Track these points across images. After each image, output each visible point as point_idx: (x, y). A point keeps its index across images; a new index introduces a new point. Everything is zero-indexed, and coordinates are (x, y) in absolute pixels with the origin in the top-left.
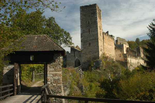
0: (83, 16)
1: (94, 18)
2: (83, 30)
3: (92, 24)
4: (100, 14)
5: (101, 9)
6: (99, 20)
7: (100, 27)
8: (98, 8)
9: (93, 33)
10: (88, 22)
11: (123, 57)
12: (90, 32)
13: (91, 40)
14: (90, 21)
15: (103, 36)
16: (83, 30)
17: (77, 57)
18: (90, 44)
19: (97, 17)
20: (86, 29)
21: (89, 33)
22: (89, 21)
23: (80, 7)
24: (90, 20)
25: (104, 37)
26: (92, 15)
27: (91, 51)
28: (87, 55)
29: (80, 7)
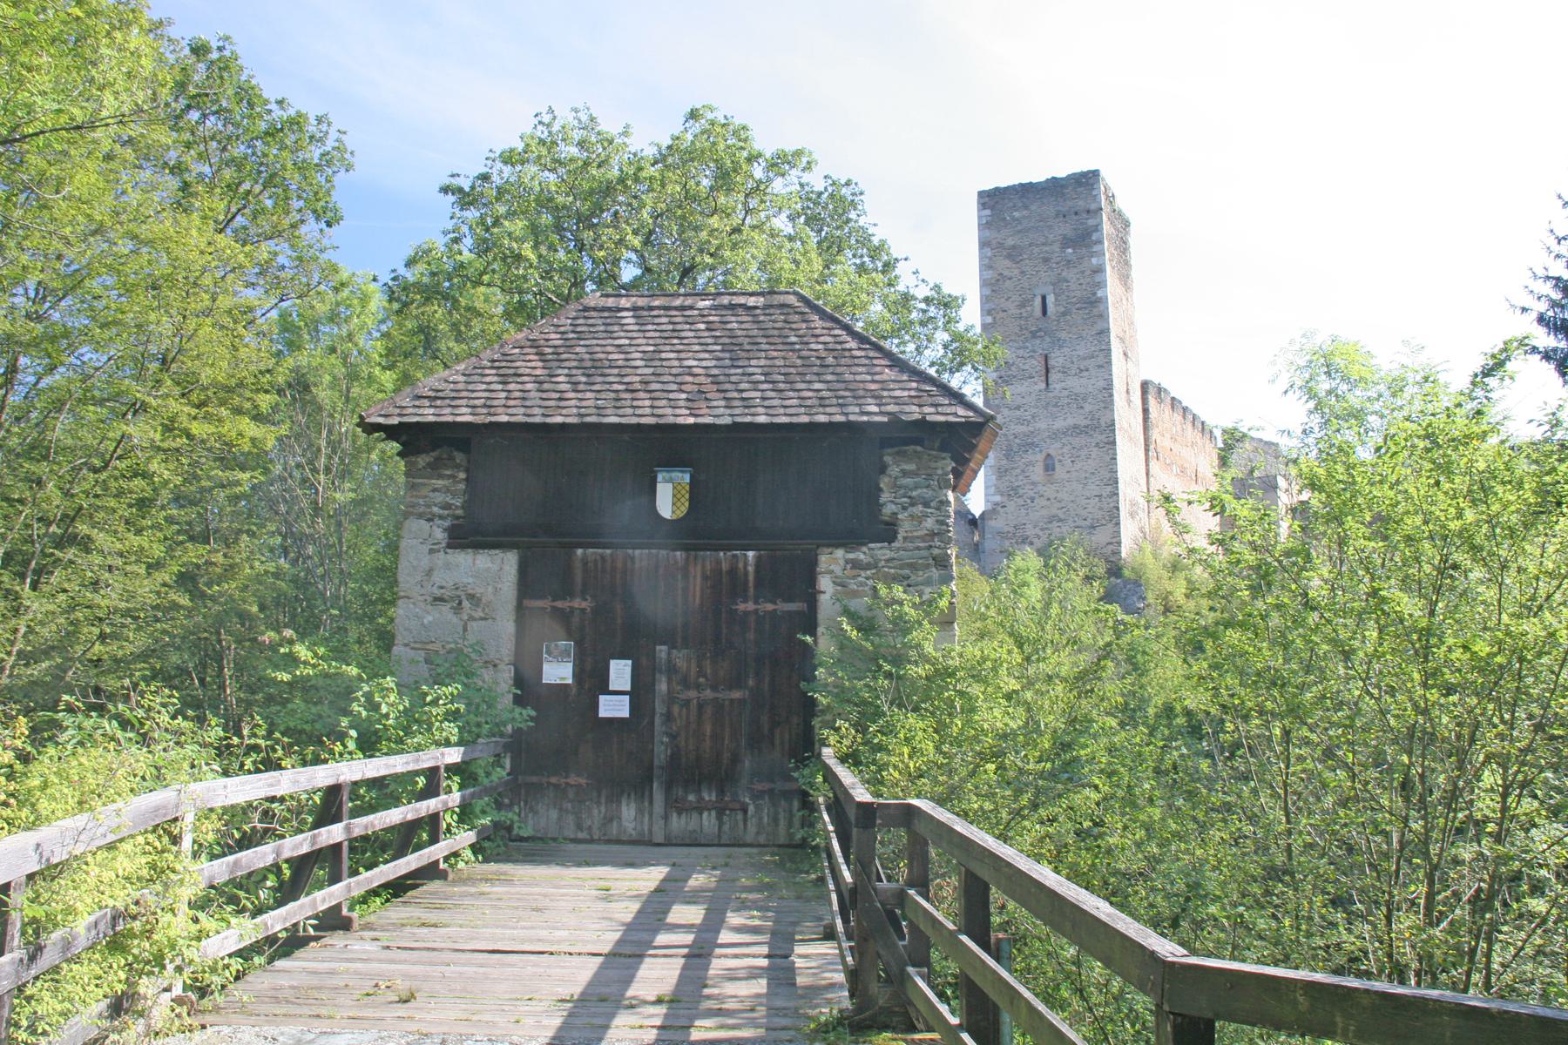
0: (1003, 264)
1: (1083, 272)
3: (1064, 314)
4: (1123, 247)
5: (1128, 213)
7: (1122, 340)
8: (1111, 199)
9: (1072, 382)
10: (1038, 301)
12: (1053, 377)
13: (1055, 435)
14: (1050, 299)
15: (1146, 411)
19: (1099, 270)
20: (1021, 352)
21: (1043, 386)
22: (1044, 298)
23: (981, 194)
26: (1070, 250)
27: (1060, 514)
29: (981, 194)
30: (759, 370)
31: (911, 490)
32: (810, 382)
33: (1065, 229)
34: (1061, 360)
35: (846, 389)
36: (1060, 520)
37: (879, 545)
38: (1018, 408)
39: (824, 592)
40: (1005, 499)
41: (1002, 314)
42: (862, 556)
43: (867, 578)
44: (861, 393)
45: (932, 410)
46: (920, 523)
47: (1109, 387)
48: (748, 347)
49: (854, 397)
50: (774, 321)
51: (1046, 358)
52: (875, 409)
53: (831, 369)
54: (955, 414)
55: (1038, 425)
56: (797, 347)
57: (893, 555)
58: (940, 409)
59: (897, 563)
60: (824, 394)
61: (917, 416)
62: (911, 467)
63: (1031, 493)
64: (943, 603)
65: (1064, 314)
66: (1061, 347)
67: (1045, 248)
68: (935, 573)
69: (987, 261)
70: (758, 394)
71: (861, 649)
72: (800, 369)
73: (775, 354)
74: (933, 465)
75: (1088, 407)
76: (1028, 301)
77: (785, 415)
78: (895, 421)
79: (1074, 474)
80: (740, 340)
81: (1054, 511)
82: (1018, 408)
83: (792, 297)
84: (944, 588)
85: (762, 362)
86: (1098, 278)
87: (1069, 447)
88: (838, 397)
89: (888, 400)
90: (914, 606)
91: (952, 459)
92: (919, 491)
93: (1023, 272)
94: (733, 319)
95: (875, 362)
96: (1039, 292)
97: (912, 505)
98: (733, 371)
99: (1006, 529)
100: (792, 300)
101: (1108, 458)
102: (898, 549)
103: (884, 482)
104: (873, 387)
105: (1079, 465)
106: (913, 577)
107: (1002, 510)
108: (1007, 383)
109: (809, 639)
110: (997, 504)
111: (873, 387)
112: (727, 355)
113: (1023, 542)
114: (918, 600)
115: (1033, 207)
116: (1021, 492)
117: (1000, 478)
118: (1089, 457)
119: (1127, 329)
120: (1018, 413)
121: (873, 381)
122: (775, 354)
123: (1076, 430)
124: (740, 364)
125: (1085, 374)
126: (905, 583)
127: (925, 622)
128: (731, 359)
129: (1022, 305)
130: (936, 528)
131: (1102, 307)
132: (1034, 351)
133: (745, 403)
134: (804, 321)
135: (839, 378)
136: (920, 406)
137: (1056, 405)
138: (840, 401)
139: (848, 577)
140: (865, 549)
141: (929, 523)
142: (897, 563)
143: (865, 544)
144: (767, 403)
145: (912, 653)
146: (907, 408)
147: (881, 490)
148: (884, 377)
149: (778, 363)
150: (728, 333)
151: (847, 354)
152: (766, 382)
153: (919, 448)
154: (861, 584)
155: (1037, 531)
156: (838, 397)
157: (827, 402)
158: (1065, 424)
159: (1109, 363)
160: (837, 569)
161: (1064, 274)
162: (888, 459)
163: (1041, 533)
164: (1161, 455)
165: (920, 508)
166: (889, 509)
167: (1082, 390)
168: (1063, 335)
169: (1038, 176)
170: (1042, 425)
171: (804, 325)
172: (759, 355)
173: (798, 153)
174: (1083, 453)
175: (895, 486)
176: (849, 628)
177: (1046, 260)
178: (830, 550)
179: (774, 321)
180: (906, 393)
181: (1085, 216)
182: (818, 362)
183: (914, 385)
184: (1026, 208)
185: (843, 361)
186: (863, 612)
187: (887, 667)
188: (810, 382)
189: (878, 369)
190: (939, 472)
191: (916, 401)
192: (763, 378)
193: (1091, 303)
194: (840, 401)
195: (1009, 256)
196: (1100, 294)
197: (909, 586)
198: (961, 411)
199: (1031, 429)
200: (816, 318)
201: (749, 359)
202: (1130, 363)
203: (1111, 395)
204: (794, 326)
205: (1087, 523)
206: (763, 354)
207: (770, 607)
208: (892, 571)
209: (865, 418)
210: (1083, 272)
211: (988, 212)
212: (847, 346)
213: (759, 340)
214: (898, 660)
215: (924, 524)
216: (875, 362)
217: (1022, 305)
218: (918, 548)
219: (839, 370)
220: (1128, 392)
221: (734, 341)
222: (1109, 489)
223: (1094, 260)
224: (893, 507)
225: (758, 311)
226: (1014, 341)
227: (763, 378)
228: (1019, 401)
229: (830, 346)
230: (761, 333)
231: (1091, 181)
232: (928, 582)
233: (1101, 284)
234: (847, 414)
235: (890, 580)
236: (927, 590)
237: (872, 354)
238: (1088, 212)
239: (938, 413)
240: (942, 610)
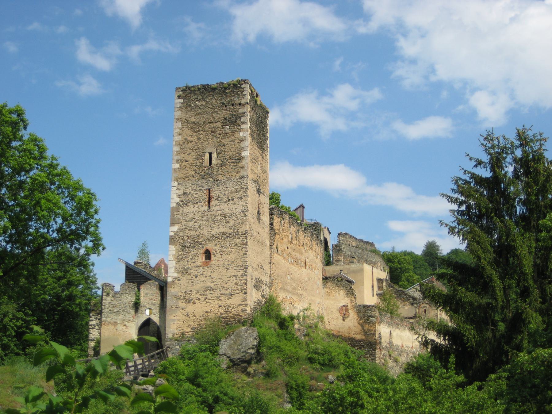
0: (187, 132)
1: (233, 141)
2: (185, 193)
7: (256, 182)
10: (207, 156)
11: (356, 317)
12: (213, 203)
14: (214, 155)
15: (271, 224)
16: (185, 193)
17: (147, 312)
18: (208, 254)
20: (195, 187)
21: (207, 208)
22: (210, 154)
24: (213, 150)
26: (228, 127)
27: (212, 285)
28: (194, 303)
33: (224, 113)
34: (218, 193)
36: (212, 290)
38: (191, 220)
40: (180, 275)
41: (185, 163)
51: (209, 190)
55: (202, 232)
63: (196, 273)
75: (232, 222)
79: (222, 262)
81: (209, 284)
82: (191, 220)
93: (199, 138)
99: (180, 294)
105: (224, 257)
108: (185, 205)
110: (175, 278)
113: (189, 302)
116: (190, 271)
117: (178, 262)
120: (191, 223)
125: (231, 202)
137: (213, 220)
155: (198, 295)
158: (218, 231)
163: (200, 297)
164: (280, 252)
167: (229, 212)
168: (220, 178)
170: (204, 232)
177: (213, 132)
184: (204, 99)
199: (198, 234)
205: (228, 292)
210: (233, 141)
222: (242, 272)
228: (191, 216)
231: (243, 86)
238: (240, 104)
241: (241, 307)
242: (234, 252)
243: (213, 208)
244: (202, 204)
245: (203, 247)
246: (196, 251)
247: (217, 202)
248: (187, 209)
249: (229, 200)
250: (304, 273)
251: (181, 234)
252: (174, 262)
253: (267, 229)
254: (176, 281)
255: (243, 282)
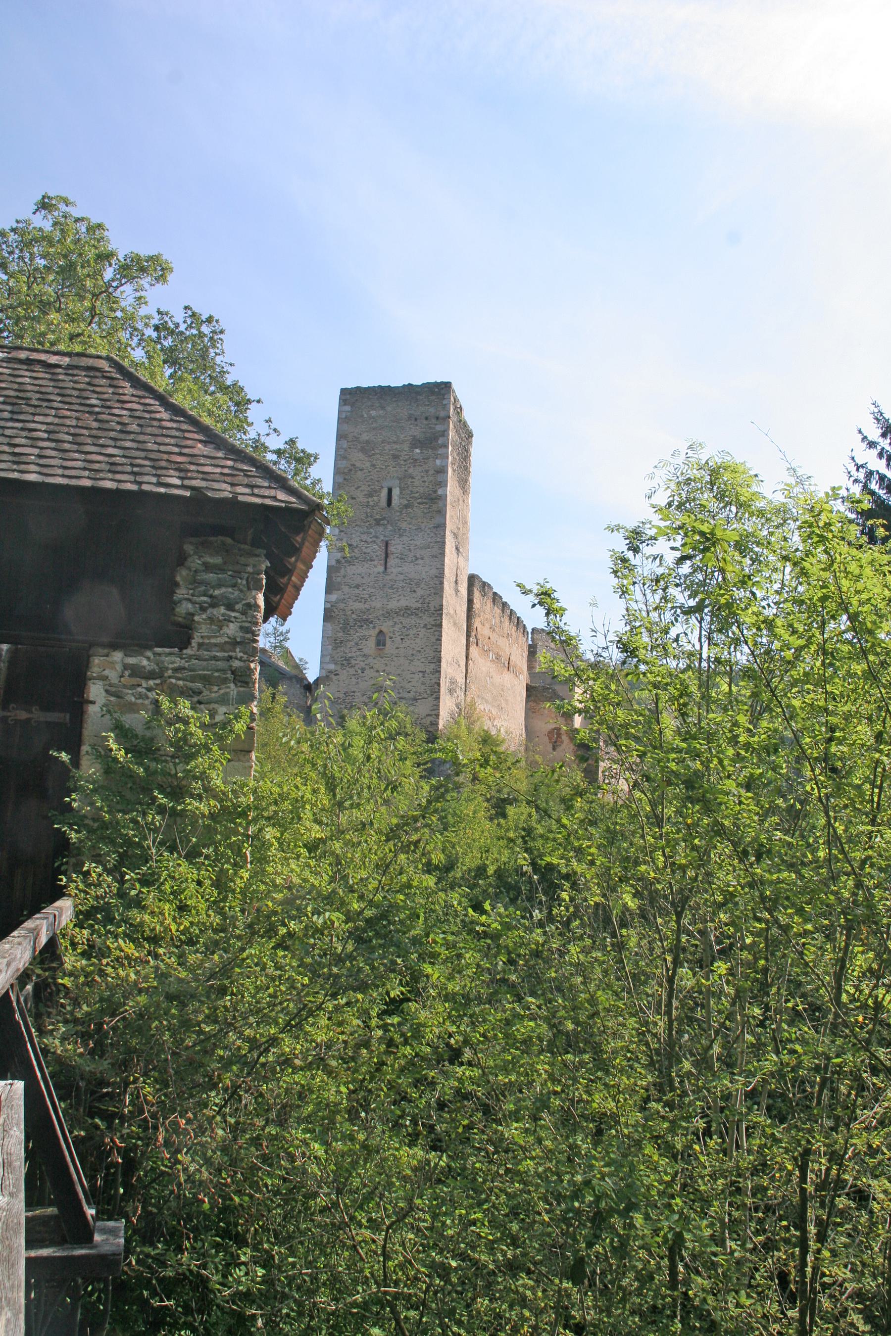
0: (357, 457)
1: (427, 471)
4: (465, 455)
6: (458, 492)
7: (456, 536)
8: (459, 410)
10: (384, 492)
12: (392, 562)
13: (389, 614)
14: (396, 492)
15: (470, 602)
19: (442, 471)
20: (364, 537)
21: (381, 569)
22: (390, 491)
23: (344, 391)
25: (477, 605)
26: (418, 451)
29: (344, 391)
30: (44, 427)
31: (214, 588)
32: (103, 446)
33: (416, 431)
34: (400, 547)
35: (146, 458)
37: (167, 650)
38: (357, 586)
39: (93, 703)
40: (338, 668)
42: (145, 662)
43: (149, 689)
44: (163, 464)
45: (247, 491)
46: (221, 628)
47: (440, 576)
48: (36, 403)
49: (153, 467)
50: (75, 382)
51: (387, 545)
52: (178, 482)
53: (132, 436)
54: (274, 498)
55: (374, 604)
56: (97, 409)
57: (183, 663)
58: (256, 491)
59: (187, 674)
60: (117, 460)
61: (226, 494)
62: (217, 560)
64: (240, 727)
65: (407, 506)
66: (401, 535)
67: (398, 447)
68: (233, 690)
69: (342, 452)
70: (36, 451)
71: (131, 775)
72: (94, 432)
73: (68, 413)
74: (243, 560)
75: (420, 592)
76: (376, 491)
77: (63, 476)
78: (199, 499)
80: (29, 395)
82: (357, 586)
83: (104, 362)
84: (242, 709)
85: (49, 420)
86: (440, 478)
87: (400, 626)
88: (132, 465)
89: (195, 475)
90: (203, 726)
91: (268, 557)
92: (223, 590)
93: (373, 465)
94: (27, 374)
95: (187, 435)
96: (386, 484)
97: (213, 605)
98: (10, 424)
100: (104, 365)
101: (433, 639)
102: (190, 657)
103: (181, 576)
104: (179, 459)
105: (407, 642)
106: (206, 693)
107: (335, 678)
109: (64, 756)
110: (330, 672)
111: (179, 459)
112: (9, 408)
114: (207, 719)
115: (389, 409)
116: (353, 662)
117: (335, 648)
118: (417, 635)
119: (461, 526)
120: (357, 591)
121: (181, 454)
122: (68, 413)
123: (407, 611)
124: (21, 417)
125: (420, 562)
126: (195, 699)
127: (215, 748)
128: (11, 412)
129: (370, 495)
130: (239, 636)
131: (441, 504)
132: (377, 537)
133: (16, 459)
134: (111, 386)
135: (140, 446)
136: (233, 485)
137: (391, 587)
138: (135, 469)
139: (125, 686)
140: (149, 654)
141: (232, 629)
142: (187, 674)
143: (150, 648)
144: (42, 461)
145: (197, 786)
146: (216, 486)
147: (177, 585)
148: (195, 451)
149: (68, 422)
150: (16, 386)
151: (155, 423)
152: (48, 439)
153: (229, 541)
154: (140, 696)
156: (132, 465)
157: (119, 468)
159: (443, 554)
160: (113, 675)
161: (411, 471)
162: (189, 548)
164: (480, 642)
165: (222, 610)
166: (185, 607)
168: (404, 525)
169: (397, 382)
170: (378, 605)
171: (111, 390)
172: (48, 411)
173: (154, 259)
174: (411, 632)
175: (195, 582)
176: (114, 746)
177: (396, 457)
178: (106, 651)
179: (75, 382)
180: (218, 470)
181: (434, 421)
182: (118, 428)
183: (230, 463)
184: (383, 408)
185: (149, 430)
186: (140, 730)
187: (162, 799)
188: (103, 446)
189: (189, 443)
190: (250, 569)
191: (228, 479)
192: (46, 436)
193: (432, 499)
194: (135, 469)
195: (363, 450)
196: (440, 492)
197: (200, 703)
198: (281, 496)
200: (128, 385)
201: (34, 414)
202: (461, 558)
203: (442, 583)
204: (98, 389)
205: (412, 695)
206: (53, 412)
207: (23, 715)
208: (181, 683)
209: (162, 490)
210: (427, 471)
211: (348, 408)
212: (158, 416)
213: (52, 397)
214: (178, 792)
215: (225, 630)
216: (187, 435)
217: (370, 495)
218: (215, 658)
219: (141, 438)
220: (456, 582)
221: (21, 395)
222: (433, 666)
223: (438, 462)
224: (190, 606)
225: (59, 370)
226: (360, 526)
227: (46, 436)
228: (358, 580)
229: (137, 414)
230: (57, 391)
231: (443, 392)
232: (223, 700)
233: (443, 484)
234: (140, 483)
235: (174, 693)
236: (222, 709)
237: (185, 427)
238: (437, 418)
239: (253, 495)
240: (238, 736)
241: (429, 719)
242: (421, 635)
243: (393, 570)
244: (375, 563)
245: (374, 627)
246: (366, 633)
247: (397, 560)
248: (351, 570)
249: (417, 559)
250: (507, 678)
251: (342, 606)
252: (330, 647)
253: (465, 607)
254: (332, 676)
255: (434, 681)
